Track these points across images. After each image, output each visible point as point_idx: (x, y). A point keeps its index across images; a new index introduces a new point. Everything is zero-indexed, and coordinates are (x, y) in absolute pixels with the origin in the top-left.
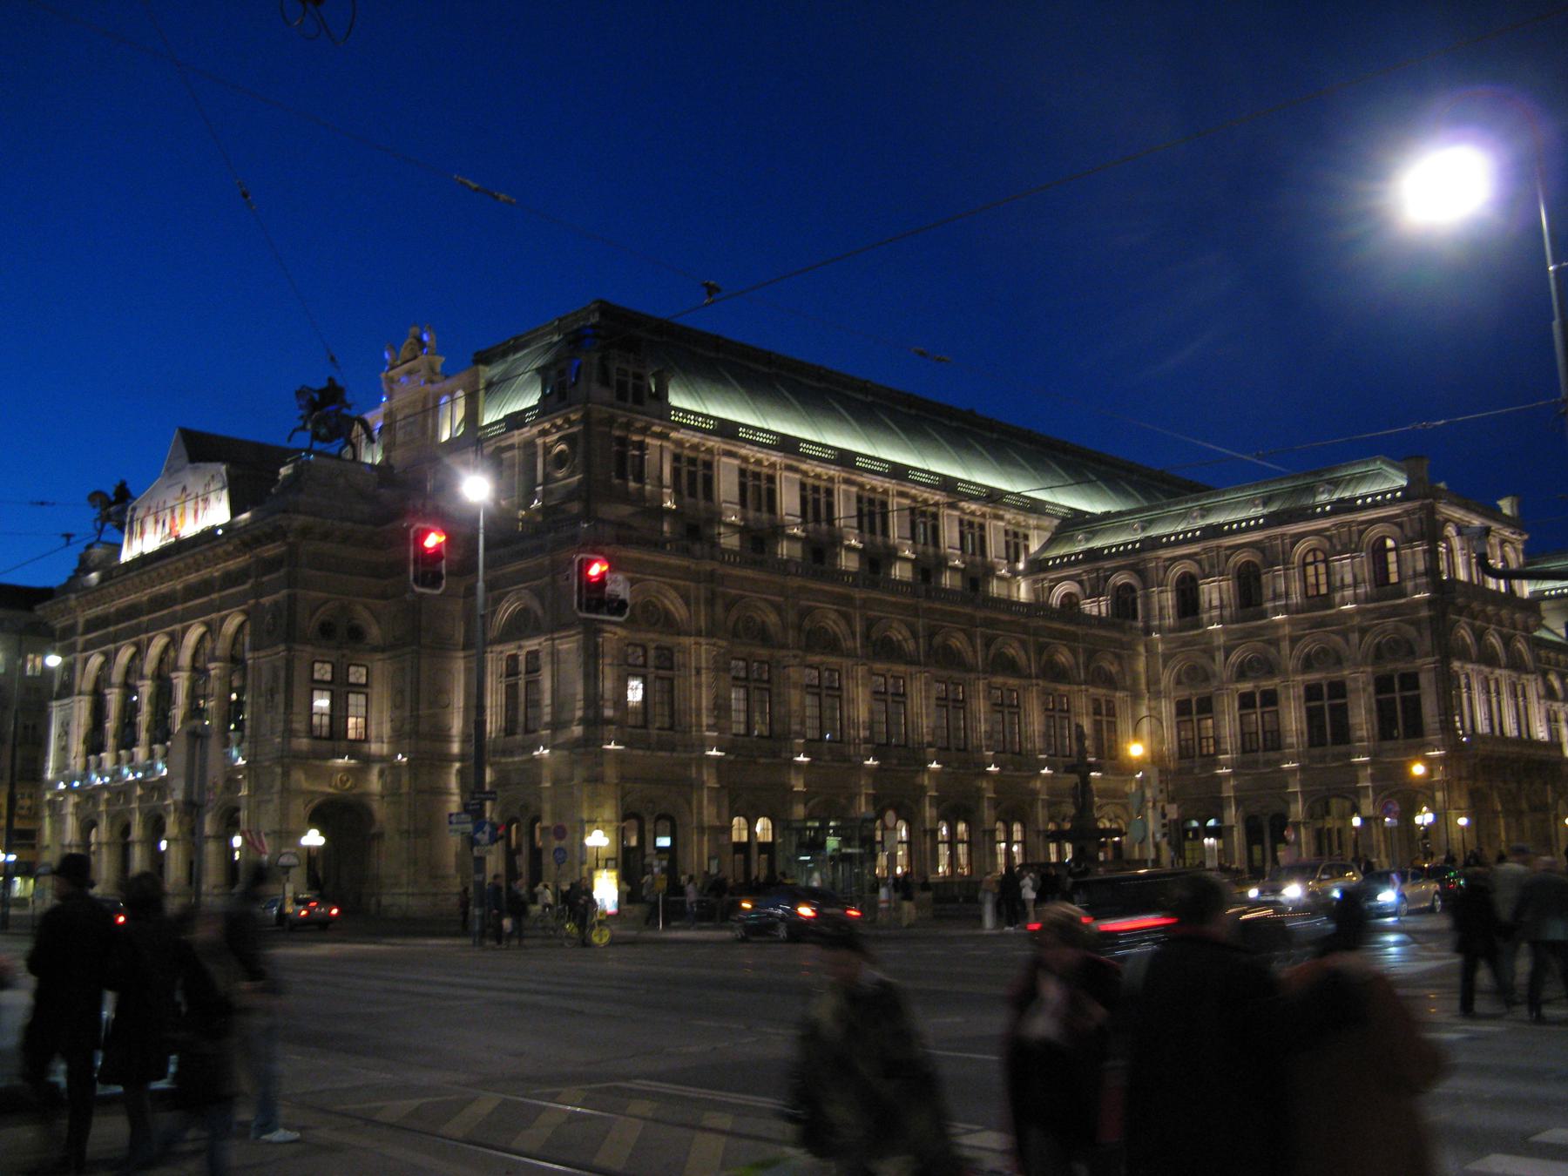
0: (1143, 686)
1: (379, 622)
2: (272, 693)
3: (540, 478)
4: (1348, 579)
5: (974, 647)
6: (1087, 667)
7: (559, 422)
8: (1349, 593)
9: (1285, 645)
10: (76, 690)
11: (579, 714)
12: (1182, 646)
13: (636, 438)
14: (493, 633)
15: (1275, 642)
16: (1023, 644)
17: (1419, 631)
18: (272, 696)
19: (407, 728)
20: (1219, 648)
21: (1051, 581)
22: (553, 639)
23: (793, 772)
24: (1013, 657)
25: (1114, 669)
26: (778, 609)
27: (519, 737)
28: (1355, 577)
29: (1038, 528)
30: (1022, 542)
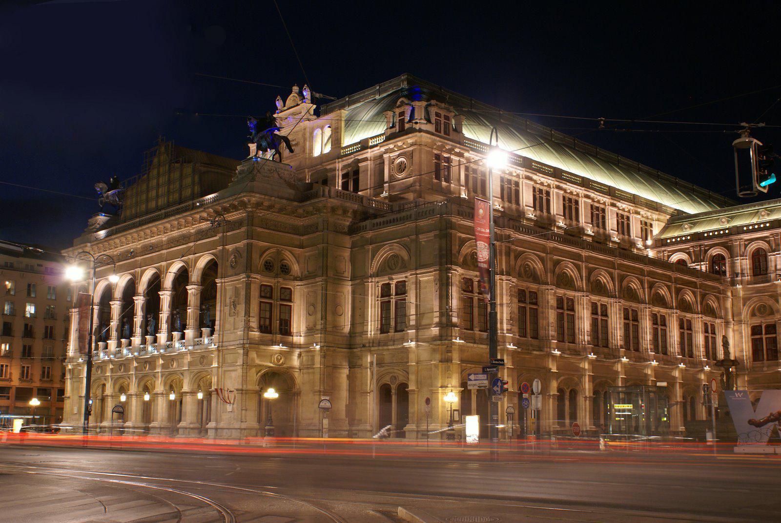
0: (730, 317)
1: (298, 262)
2: (234, 304)
3: (386, 178)
5: (644, 288)
6: (701, 304)
7: (400, 144)
11: (436, 320)
13: (446, 155)
14: (373, 269)
16: (669, 288)
18: (235, 307)
21: (669, 252)
22: (417, 274)
23: (550, 361)
24: (663, 295)
25: (715, 305)
26: (542, 260)
27: (392, 333)
29: (658, 220)
30: (649, 228)
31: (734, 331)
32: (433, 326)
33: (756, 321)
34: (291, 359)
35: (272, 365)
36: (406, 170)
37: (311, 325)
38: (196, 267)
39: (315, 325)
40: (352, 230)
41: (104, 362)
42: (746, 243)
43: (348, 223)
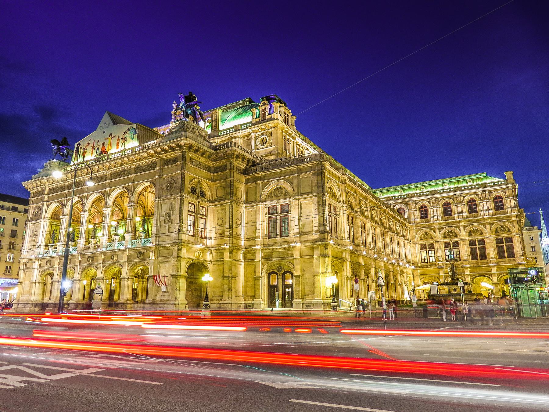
1: (210, 190)
4: (486, 208)
8: (486, 212)
9: (462, 228)
10: (43, 218)
12: (423, 228)
13: (288, 137)
14: (263, 197)
15: (459, 227)
17: (513, 224)
18: (169, 217)
19: (227, 233)
20: (437, 228)
22: (299, 199)
27: (278, 238)
28: (488, 207)
31: (411, 247)
32: (314, 232)
33: (423, 242)
34: (206, 255)
35: (195, 258)
36: (267, 142)
37: (220, 232)
38: (135, 191)
39: (223, 232)
40: (245, 172)
41: (53, 257)
42: (416, 202)
43: (243, 168)
